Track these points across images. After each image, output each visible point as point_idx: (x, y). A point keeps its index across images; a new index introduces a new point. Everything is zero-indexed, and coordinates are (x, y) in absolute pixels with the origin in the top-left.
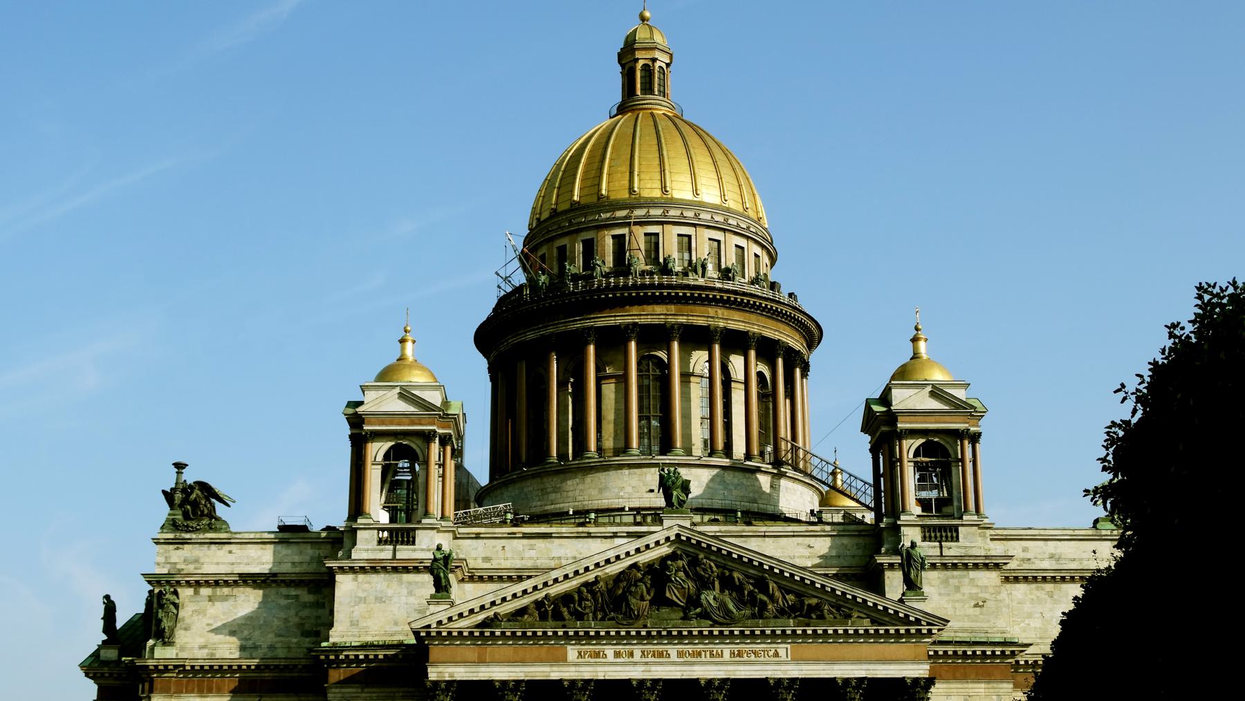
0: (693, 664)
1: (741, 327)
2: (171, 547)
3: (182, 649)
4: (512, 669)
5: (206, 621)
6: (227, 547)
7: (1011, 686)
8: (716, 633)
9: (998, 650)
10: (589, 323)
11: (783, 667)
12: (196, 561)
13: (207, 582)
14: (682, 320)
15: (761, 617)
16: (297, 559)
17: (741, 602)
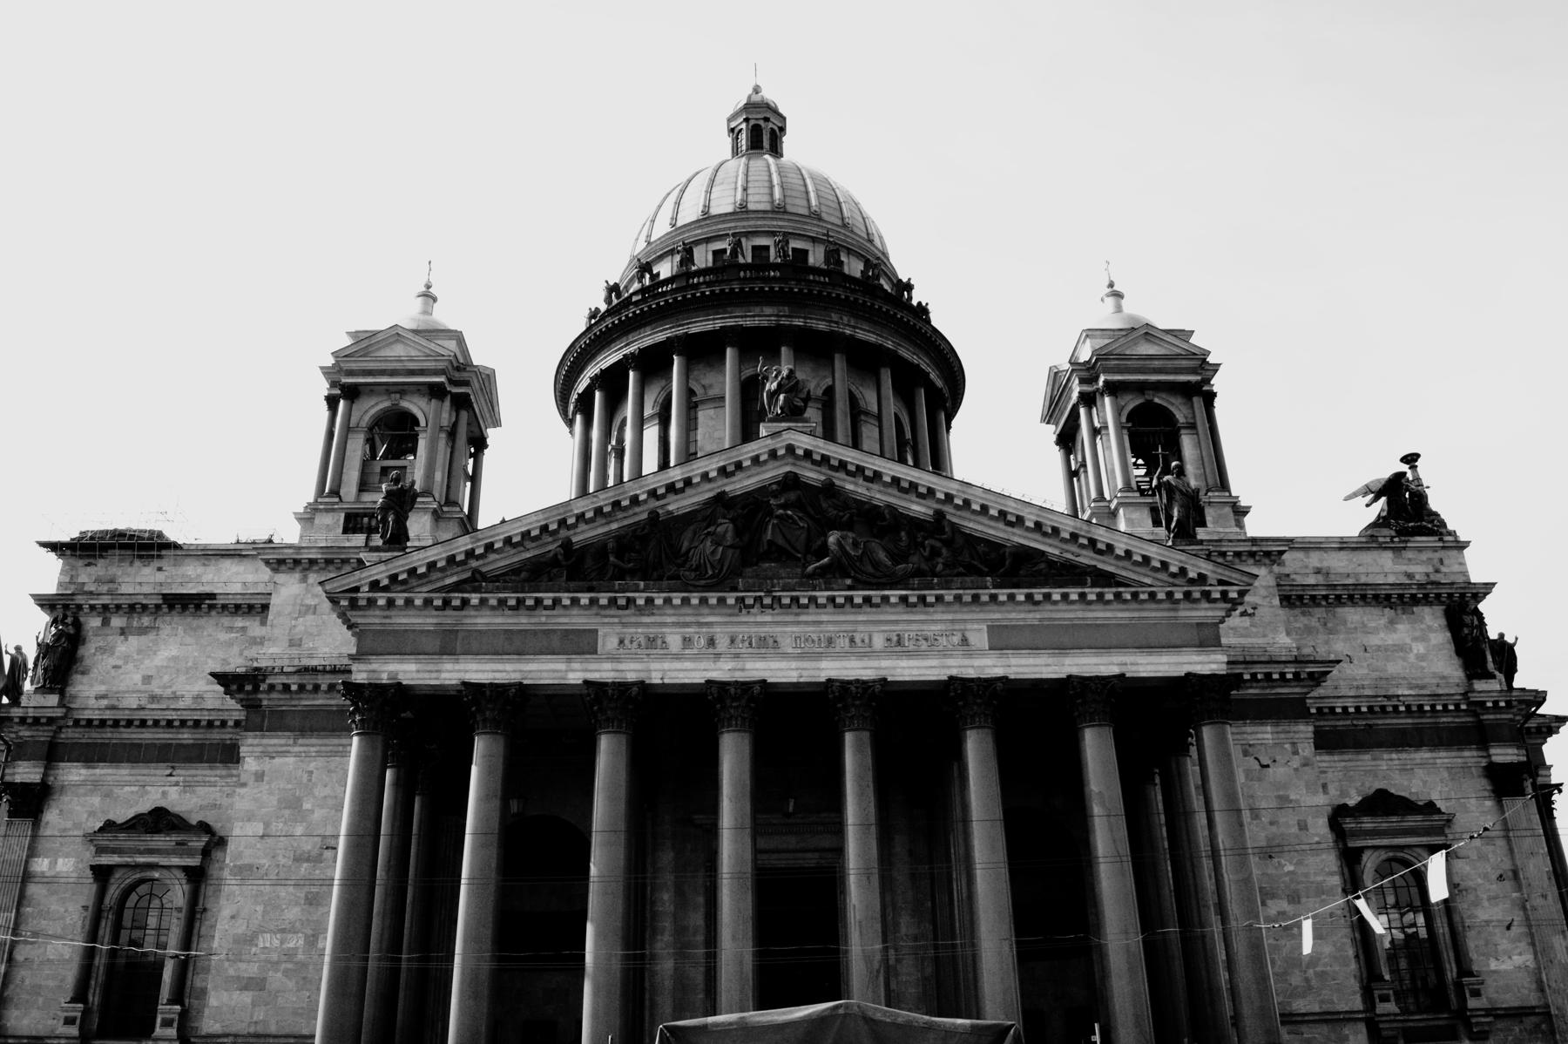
0: (818, 656)
1: (872, 338)
2: (81, 563)
3: (74, 697)
4: (500, 666)
5: (112, 661)
6: (156, 563)
7: (1311, 728)
8: (858, 600)
9: (1290, 671)
10: (680, 331)
11: (977, 662)
12: (112, 581)
13: (118, 607)
14: (798, 322)
15: (935, 575)
16: (250, 578)
17: (898, 557)
